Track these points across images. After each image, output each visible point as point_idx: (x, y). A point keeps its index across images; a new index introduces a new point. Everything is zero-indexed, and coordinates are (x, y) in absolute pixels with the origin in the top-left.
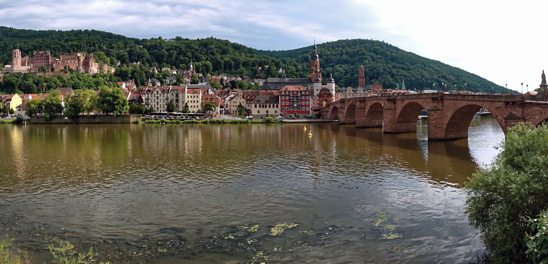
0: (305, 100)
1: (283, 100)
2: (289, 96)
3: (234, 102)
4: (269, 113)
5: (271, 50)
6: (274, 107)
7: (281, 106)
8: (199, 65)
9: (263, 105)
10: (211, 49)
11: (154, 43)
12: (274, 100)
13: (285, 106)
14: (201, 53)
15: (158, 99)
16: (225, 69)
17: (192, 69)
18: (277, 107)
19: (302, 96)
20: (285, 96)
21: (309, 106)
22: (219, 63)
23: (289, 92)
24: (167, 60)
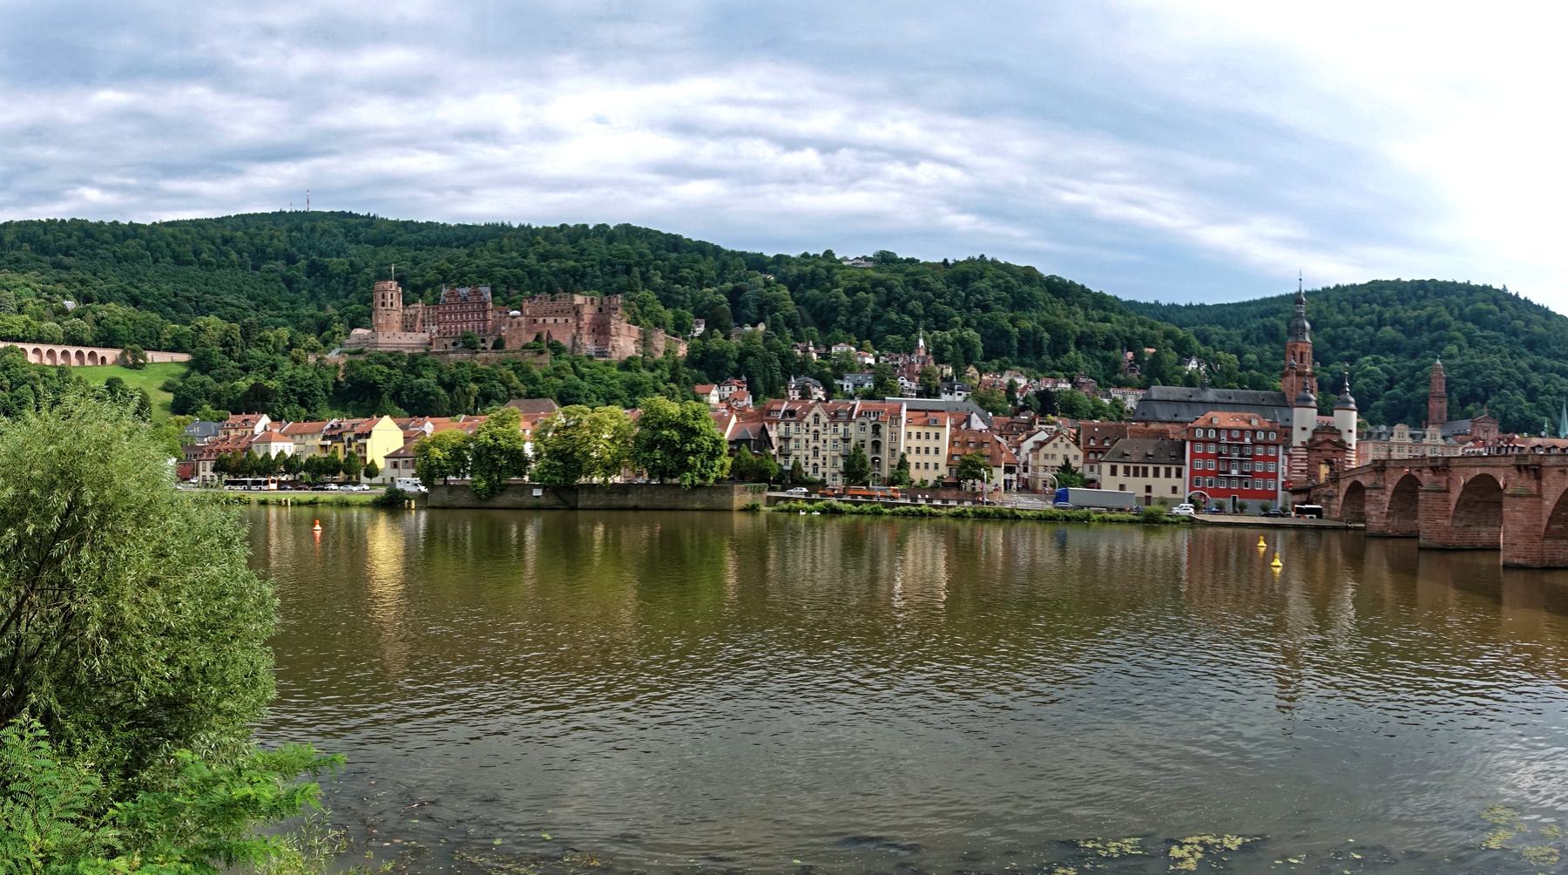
0: (1266, 458)
1: (1199, 456)
2: (1217, 442)
3: (1046, 456)
4: (1154, 494)
5: (1164, 302)
6: (1168, 475)
8: (945, 341)
9: (1136, 469)
10: (981, 293)
11: (809, 269)
12: (1174, 454)
13: (1205, 473)
14: (951, 304)
15: (816, 438)
16: (1021, 353)
17: (922, 353)
18: (1179, 475)
19: (1255, 444)
20: (1206, 442)
21: (1275, 476)
22: (1005, 334)
23: (1218, 430)
24: (848, 321)
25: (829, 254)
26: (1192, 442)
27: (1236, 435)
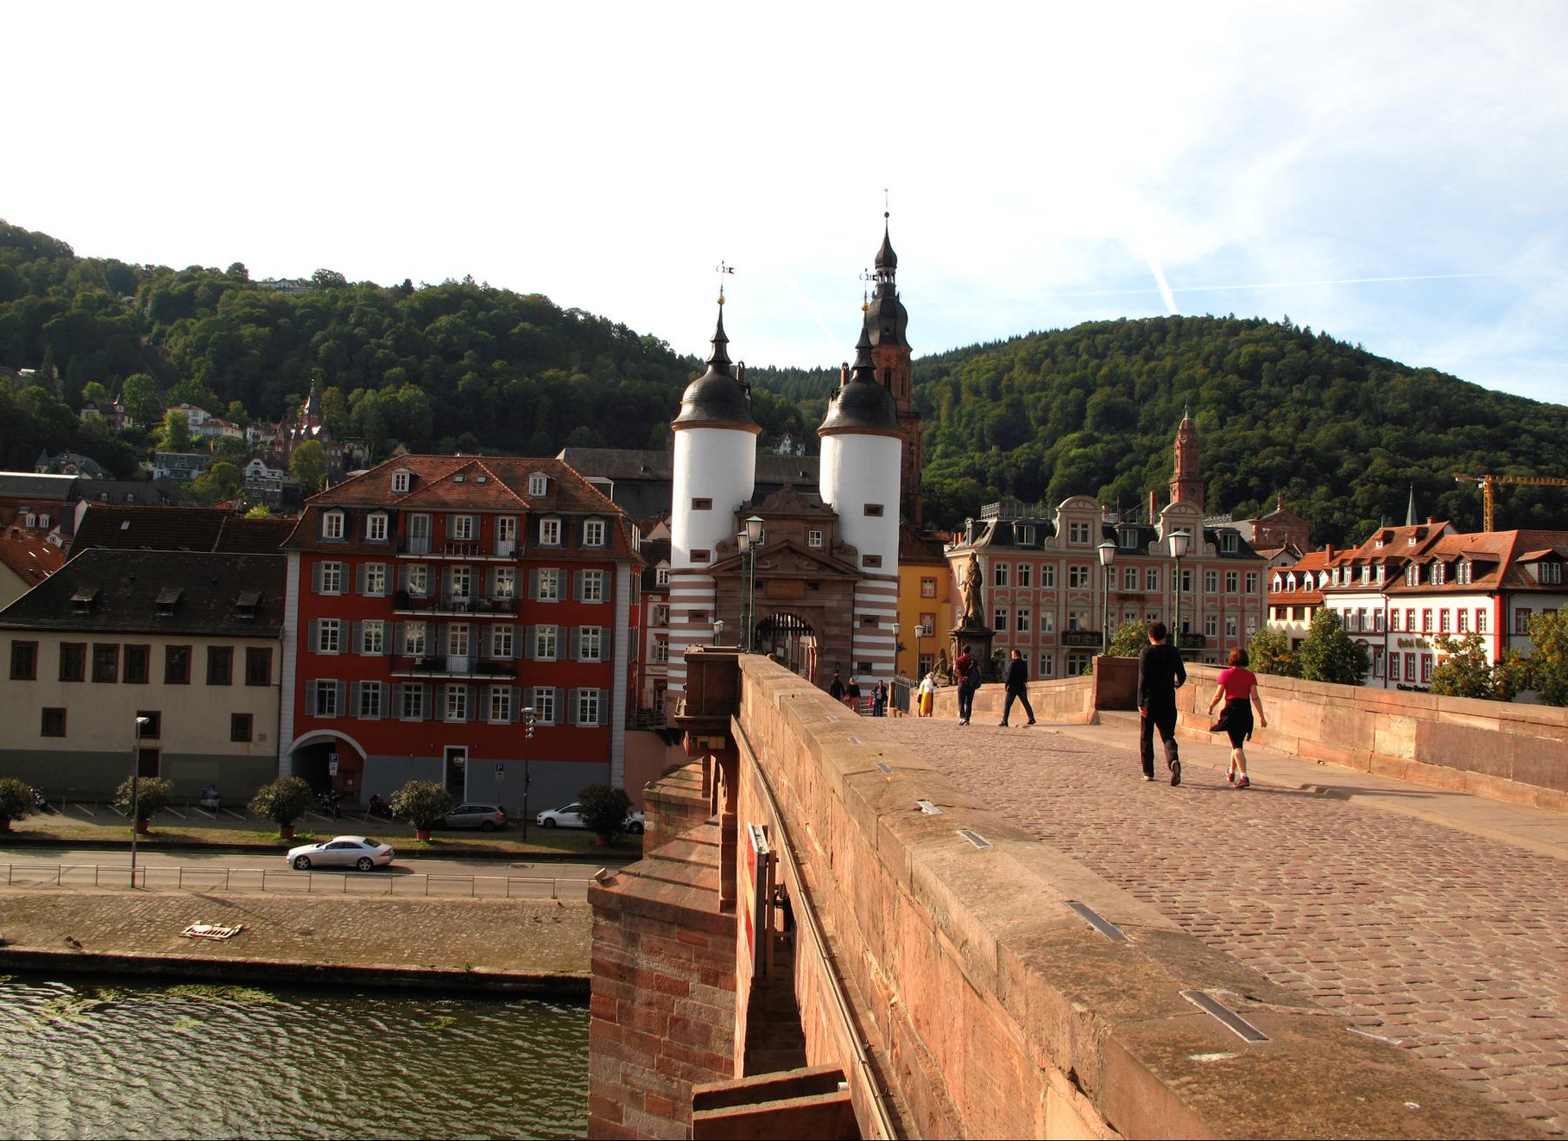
0: (569, 614)
4: (168, 743)
7: (308, 665)
9: (105, 654)
13: (350, 665)
18: (259, 673)
21: (602, 675)
25: (238, 270)
26: (311, 558)
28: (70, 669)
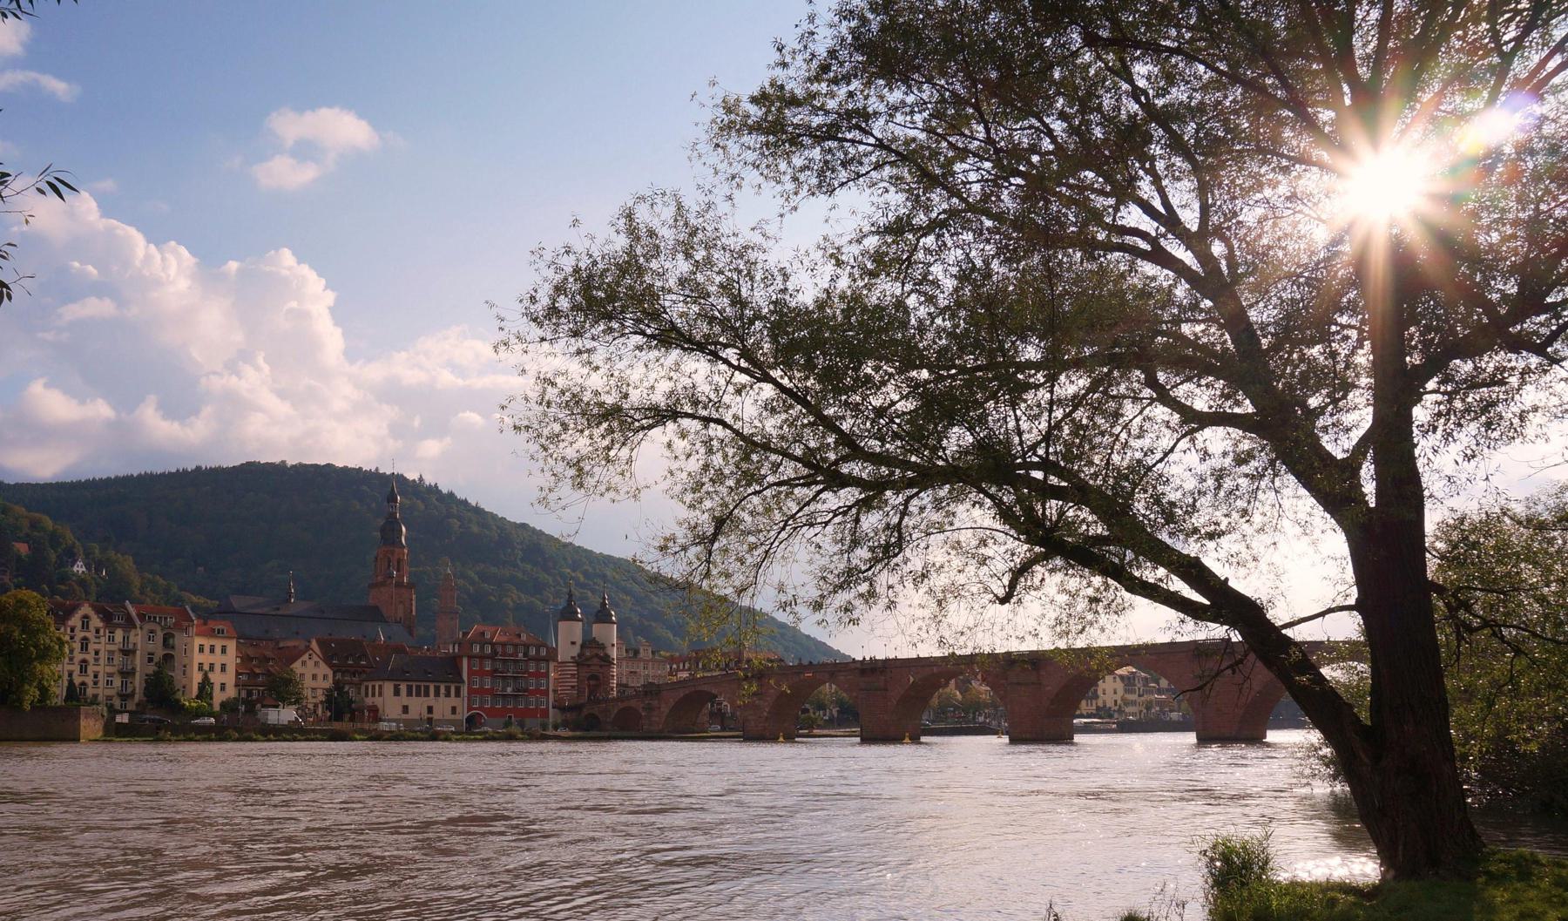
0: (538, 675)
18: (458, 694)
20: (482, 657)
26: (470, 658)
27: (510, 650)
28: (409, 694)
